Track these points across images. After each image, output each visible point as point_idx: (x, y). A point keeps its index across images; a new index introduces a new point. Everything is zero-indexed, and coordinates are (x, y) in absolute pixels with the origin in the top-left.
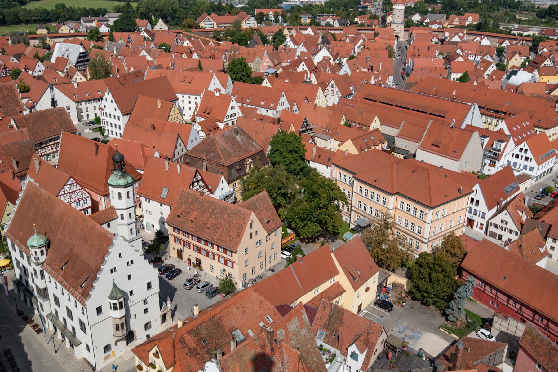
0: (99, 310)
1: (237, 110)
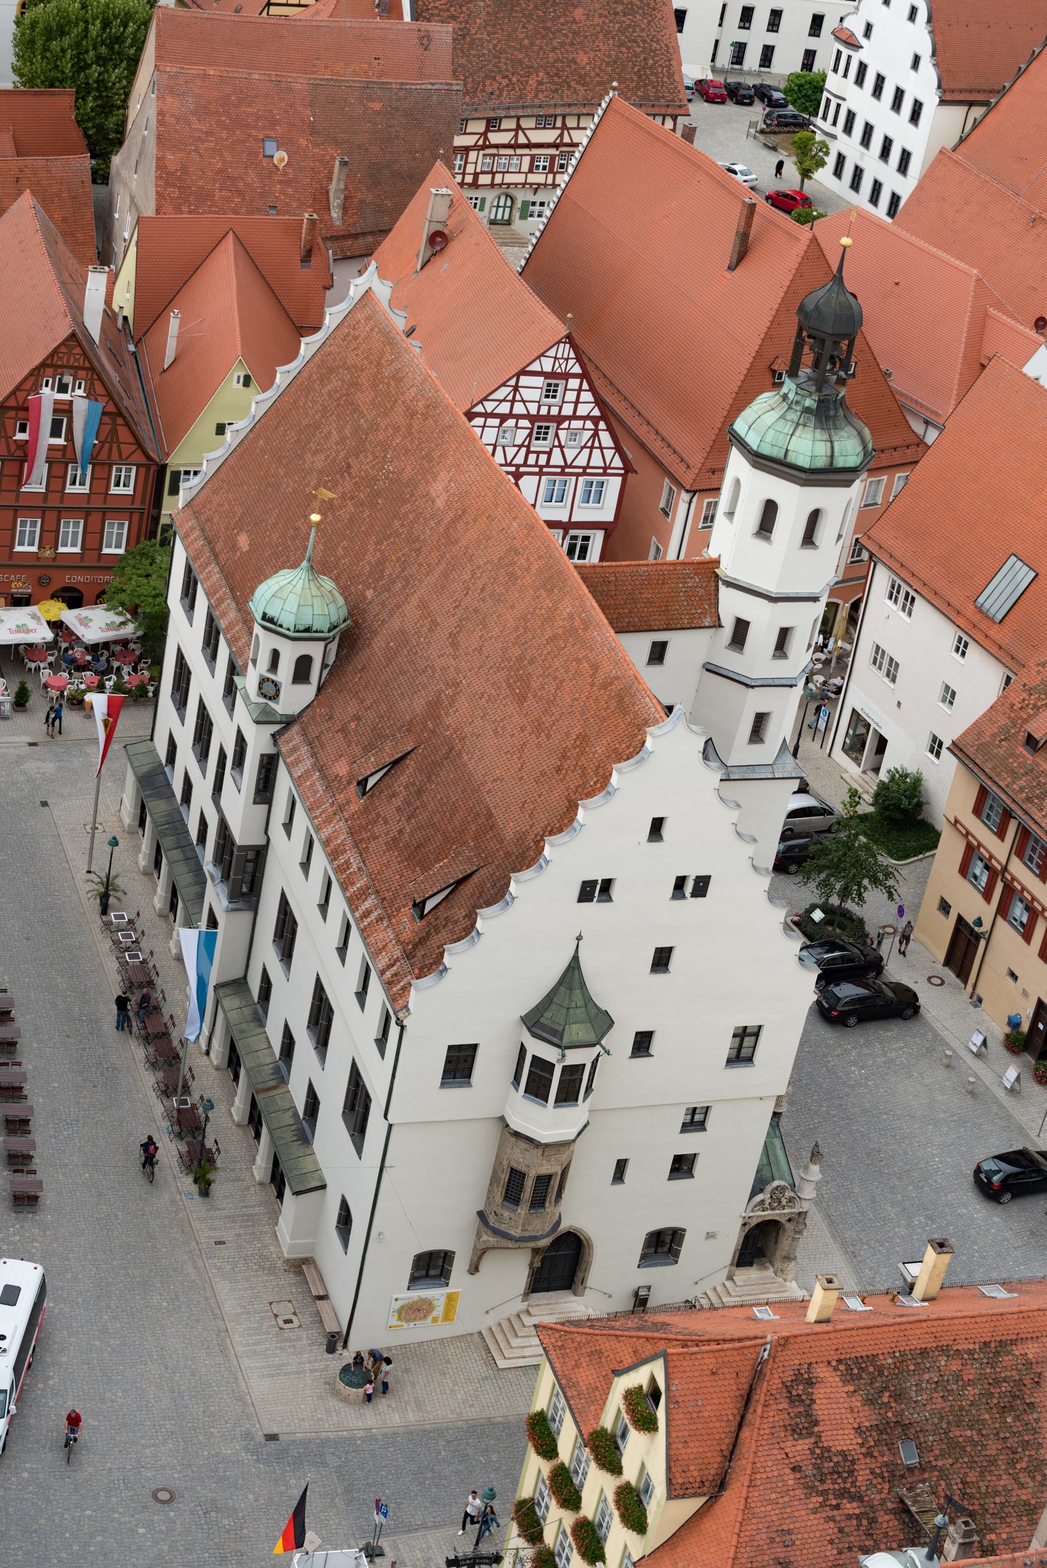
0: (460, 1064)
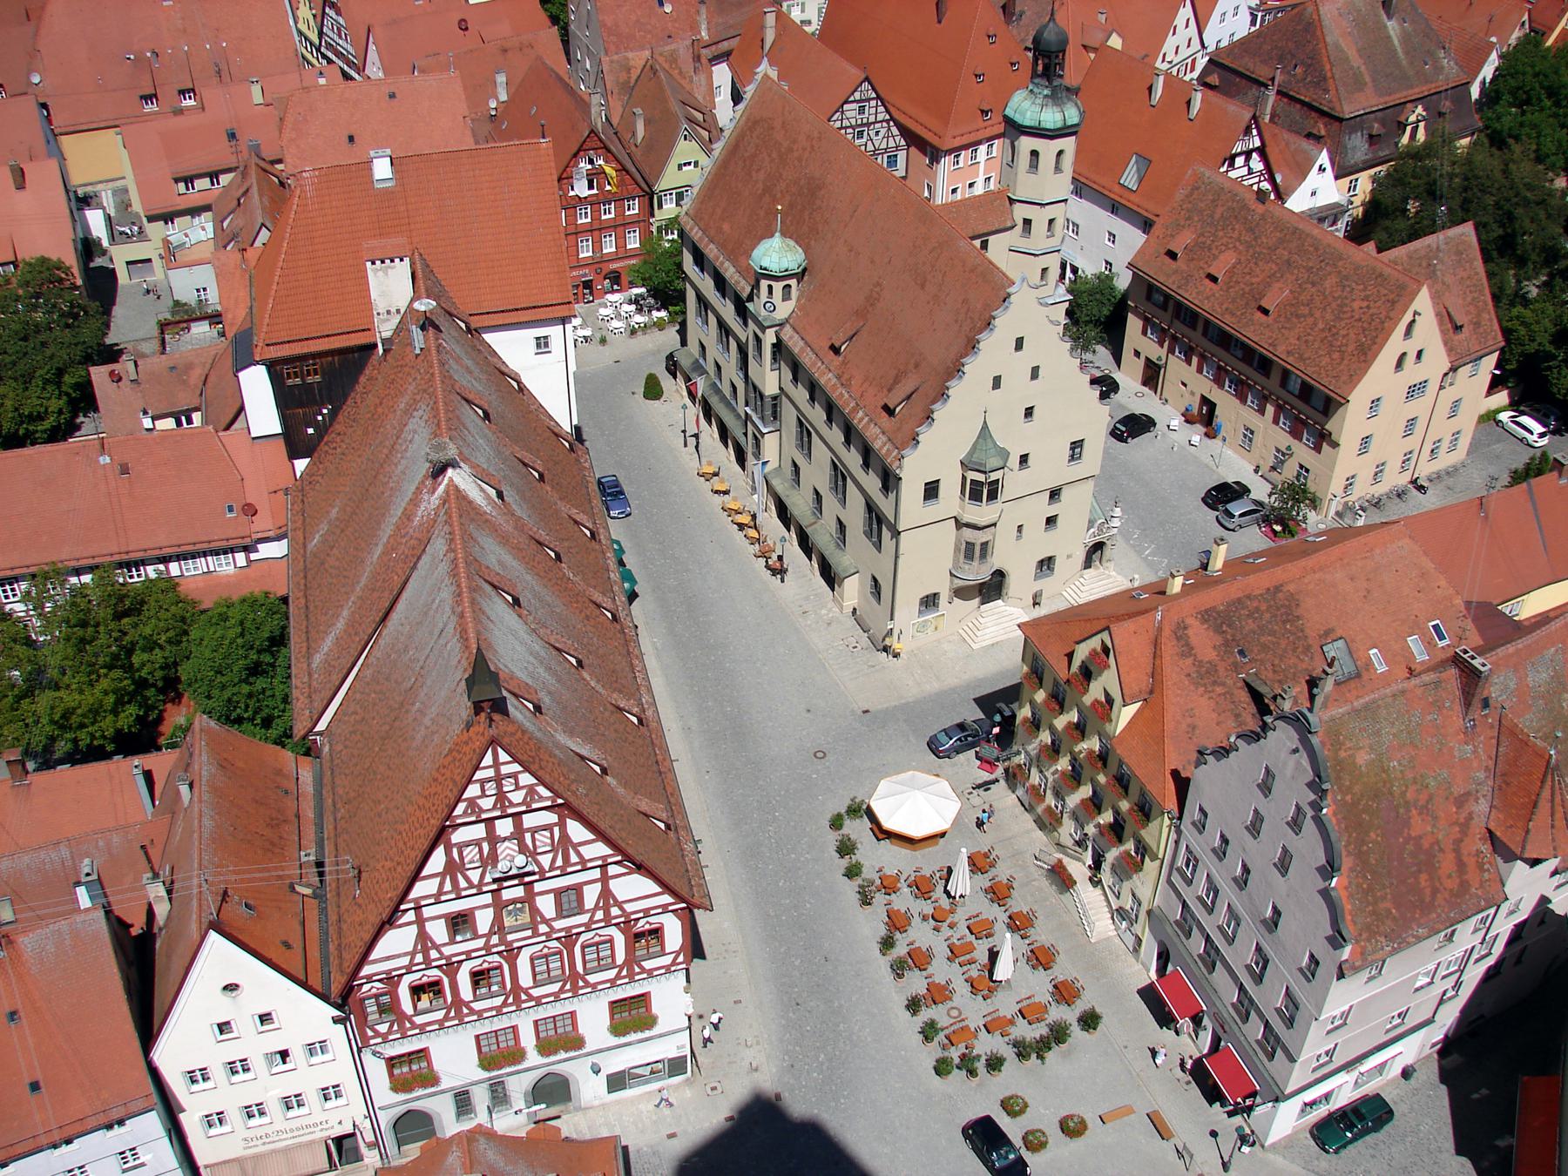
0: (931, 491)
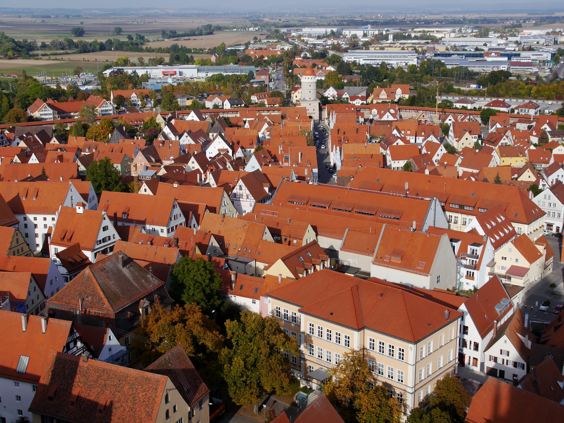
1: (112, 231)
